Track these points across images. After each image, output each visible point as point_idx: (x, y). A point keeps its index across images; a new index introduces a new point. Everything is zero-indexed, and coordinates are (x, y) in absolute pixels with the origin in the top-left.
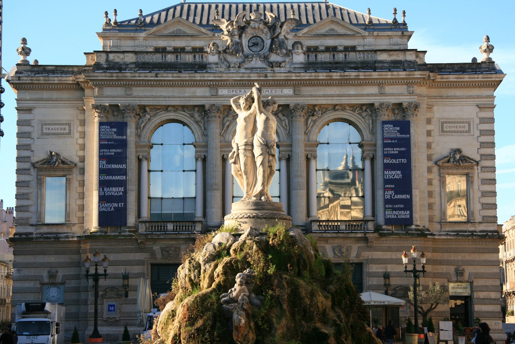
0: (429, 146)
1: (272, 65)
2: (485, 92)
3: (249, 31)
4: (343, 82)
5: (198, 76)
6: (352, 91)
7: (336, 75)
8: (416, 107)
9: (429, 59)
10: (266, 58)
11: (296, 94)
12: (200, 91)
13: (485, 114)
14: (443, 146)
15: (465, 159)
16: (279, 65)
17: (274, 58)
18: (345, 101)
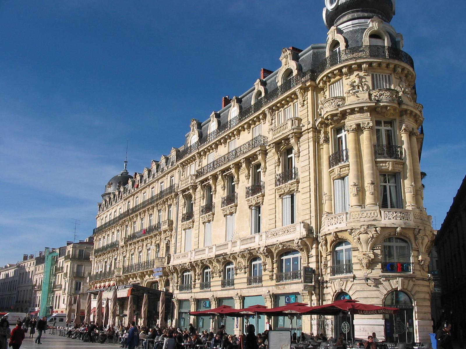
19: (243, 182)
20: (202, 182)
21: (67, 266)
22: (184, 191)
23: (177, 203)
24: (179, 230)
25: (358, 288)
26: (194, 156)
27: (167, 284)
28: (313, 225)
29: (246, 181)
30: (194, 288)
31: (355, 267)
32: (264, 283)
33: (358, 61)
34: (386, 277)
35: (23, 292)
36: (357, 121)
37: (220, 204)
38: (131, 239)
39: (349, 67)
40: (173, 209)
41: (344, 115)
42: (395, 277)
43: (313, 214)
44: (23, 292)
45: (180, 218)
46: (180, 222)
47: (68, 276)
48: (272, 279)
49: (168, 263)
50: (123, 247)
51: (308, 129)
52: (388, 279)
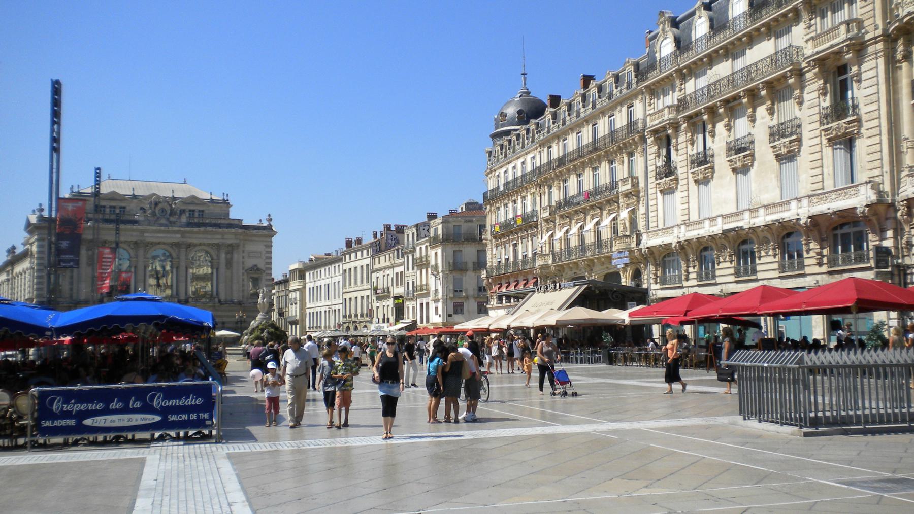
0: (243, 263)
1: (171, 222)
2: (268, 239)
3: (160, 206)
4: (206, 233)
5: (134, 227)
6: (209, 237)
7: (202, 229)
8: (238, 246)
9: (244, 223)
10: (168, 219)
11: (182, 237)
12: (134, 234)
13: (268, 250)
14: (250, 263)
15: (258, 269)
16: (174, 223)
17: (172, 219)
18: (206, 241)
19: (763, 118)
20: (689, 118)
21: (436, 254)
23: (645, 151)
26: (671, 75)
27: (637, 275)
28: (887, 187)
29: (768, 117)
30: (687, 279)
32: (808, 270)
35: (353, 300)
37: (723, 153)
40: (638, 159)
43: (886, 168)
44: (353, 300)
45: (652, 174)
46: (652, 180)
47: (440, 269)
48: (820, 264)
49: (638, 243)
51: (875, 38)
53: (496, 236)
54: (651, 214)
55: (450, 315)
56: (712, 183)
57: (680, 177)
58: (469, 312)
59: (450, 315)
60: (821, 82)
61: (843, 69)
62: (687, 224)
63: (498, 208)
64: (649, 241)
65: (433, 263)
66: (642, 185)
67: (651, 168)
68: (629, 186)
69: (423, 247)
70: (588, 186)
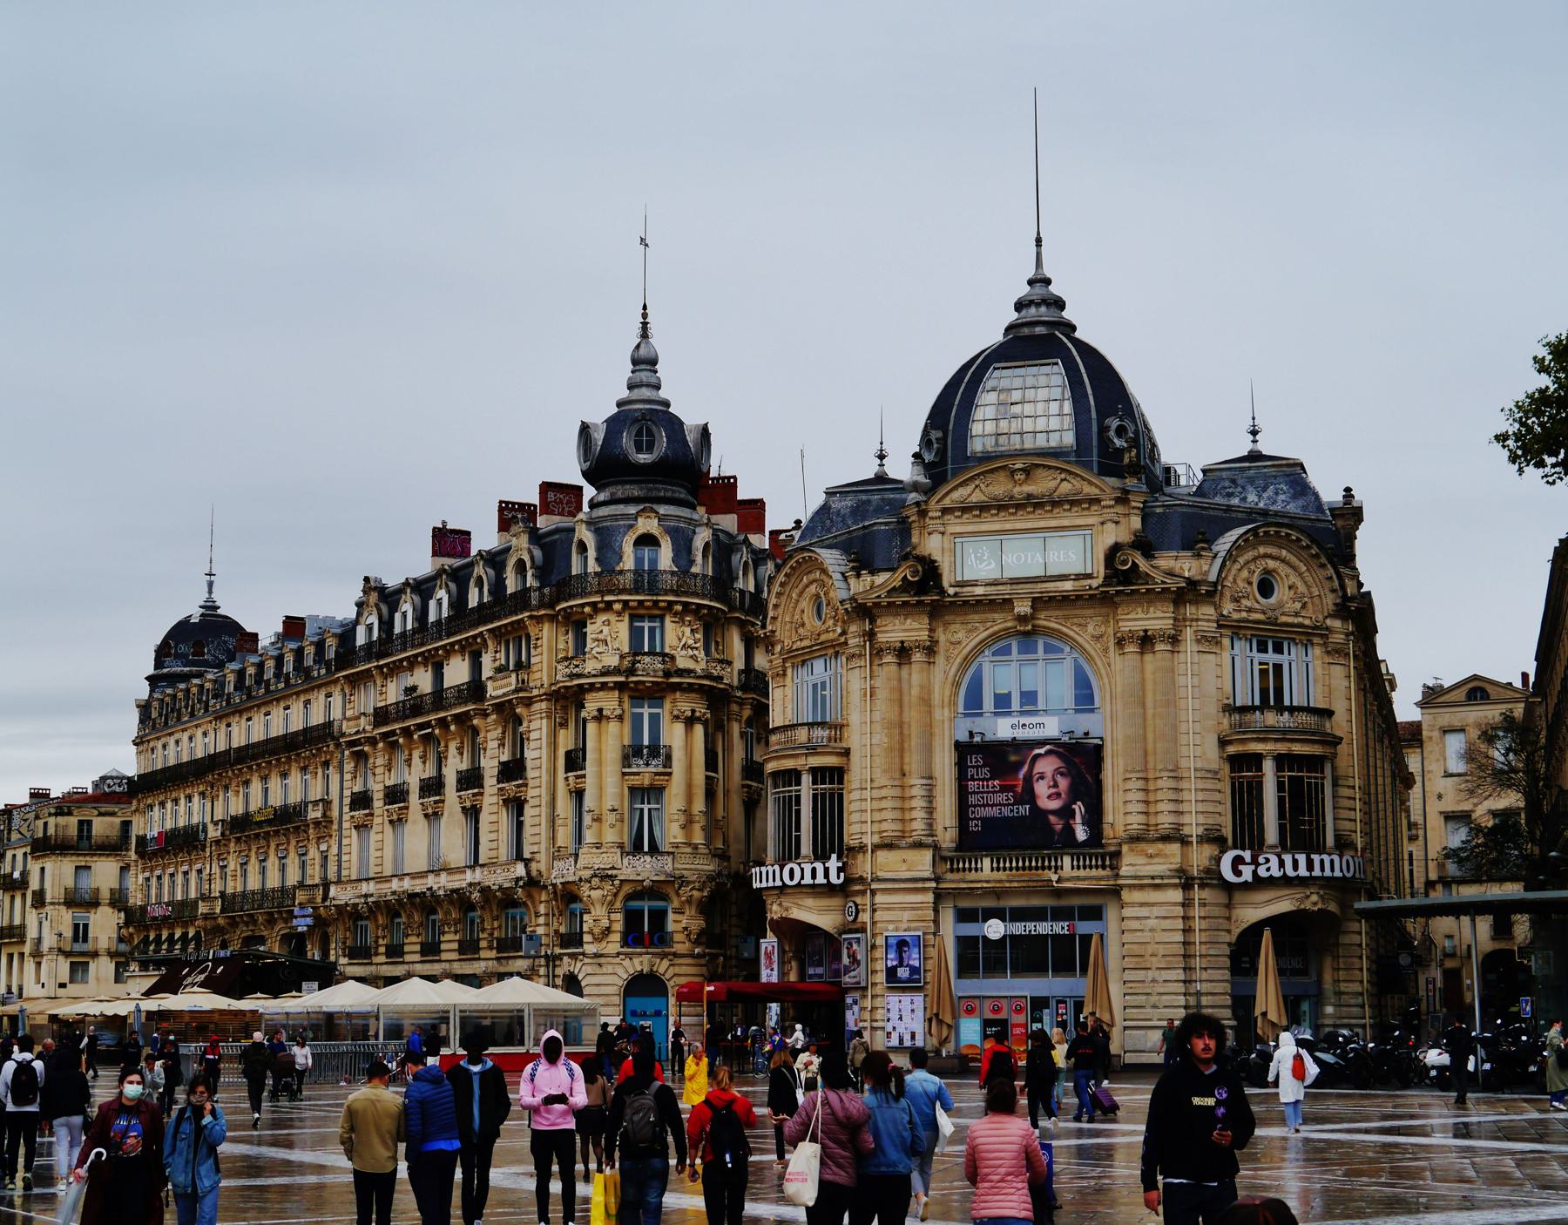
20: (385, 735)
21: (43, 869)
22: (352, 744)
23: (341, 764)
24: (346, 825)
25: (589, 969)
31: (587, 938)
32: (483, 954)
33: (607, 598)
34: (626, 954)
36: (600, 705)
38: (240, 827)
39: (594, 605)
41: (582, 690)
42: (641, 954)
45: (347, 801)
50: (217, 842)
52: (629, 956)
53: (142, 853)
54: (344, 858)
55: (63, 986)
56: (408, 827)
57: (377, 812)
58: (98, 979)
59: (63, 986)
60: (500, 730)
61: (518, 721)
62: (380, 879)
63: (151, 807)
64: (341, 895)
65: (34, 884)
66: (335, 813)
67: (347, 793)
68: (319, 814)
69: (20, 853)
70: (276, 800)
